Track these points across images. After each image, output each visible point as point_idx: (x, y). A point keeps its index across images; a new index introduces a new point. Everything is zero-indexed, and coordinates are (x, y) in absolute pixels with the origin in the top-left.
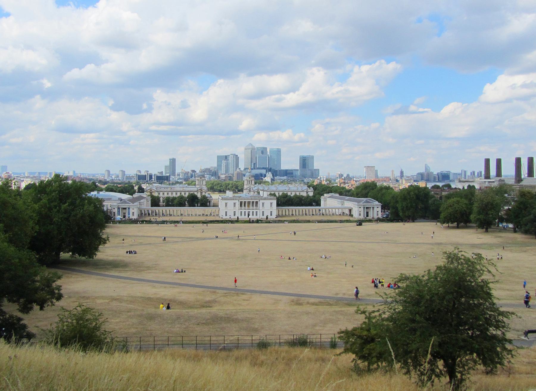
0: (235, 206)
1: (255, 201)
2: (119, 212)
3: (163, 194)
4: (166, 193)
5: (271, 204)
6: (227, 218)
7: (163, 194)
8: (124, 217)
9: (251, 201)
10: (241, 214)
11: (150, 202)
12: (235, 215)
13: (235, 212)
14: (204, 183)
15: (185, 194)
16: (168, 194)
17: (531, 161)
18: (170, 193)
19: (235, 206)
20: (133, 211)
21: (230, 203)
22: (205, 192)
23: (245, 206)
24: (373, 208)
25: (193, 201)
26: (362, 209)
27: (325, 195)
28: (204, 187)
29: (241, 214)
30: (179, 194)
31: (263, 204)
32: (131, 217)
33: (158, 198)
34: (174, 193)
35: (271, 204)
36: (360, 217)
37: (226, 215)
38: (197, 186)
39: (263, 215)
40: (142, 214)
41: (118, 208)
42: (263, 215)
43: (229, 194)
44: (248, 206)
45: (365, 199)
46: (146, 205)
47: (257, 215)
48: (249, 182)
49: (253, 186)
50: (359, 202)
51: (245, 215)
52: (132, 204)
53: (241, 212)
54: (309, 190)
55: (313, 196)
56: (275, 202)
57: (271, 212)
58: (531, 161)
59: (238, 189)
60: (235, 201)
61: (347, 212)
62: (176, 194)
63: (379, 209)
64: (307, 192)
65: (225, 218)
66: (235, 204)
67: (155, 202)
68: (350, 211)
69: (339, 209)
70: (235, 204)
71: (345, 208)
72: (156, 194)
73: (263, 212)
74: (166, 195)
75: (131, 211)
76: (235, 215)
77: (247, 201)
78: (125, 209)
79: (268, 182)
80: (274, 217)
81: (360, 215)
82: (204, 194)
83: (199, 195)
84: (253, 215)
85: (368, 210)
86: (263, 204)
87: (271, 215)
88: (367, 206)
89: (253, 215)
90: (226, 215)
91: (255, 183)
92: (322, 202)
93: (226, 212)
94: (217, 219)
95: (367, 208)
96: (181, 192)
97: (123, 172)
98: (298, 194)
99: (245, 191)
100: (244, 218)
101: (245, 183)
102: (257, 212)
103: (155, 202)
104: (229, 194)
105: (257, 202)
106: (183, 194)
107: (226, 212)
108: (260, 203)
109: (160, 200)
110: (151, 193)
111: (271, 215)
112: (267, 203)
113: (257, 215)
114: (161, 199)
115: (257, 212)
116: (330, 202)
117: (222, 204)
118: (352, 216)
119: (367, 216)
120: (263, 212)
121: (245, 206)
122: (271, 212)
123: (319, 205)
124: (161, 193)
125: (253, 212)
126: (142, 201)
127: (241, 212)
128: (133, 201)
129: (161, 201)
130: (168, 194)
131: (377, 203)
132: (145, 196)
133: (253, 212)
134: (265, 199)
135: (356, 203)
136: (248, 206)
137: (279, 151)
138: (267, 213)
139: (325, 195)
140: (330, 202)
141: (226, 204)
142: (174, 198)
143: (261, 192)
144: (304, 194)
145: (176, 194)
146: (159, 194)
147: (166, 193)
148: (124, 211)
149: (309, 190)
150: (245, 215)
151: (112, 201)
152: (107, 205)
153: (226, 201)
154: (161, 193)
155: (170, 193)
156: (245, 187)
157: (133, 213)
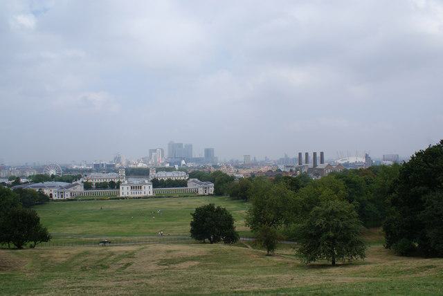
11: (83, 187)
17: (322, 154)
21: (125, 187)
25: (114, 185)
32: (66, 197)
48: (153, 171)
56: (151, 186)
58: (322, 154)
67: (87, 186)
72: (89, 181)
75: (66, 193)
80: (151, 194)
83: (116, 181)
92: (188, 184)
94: (118, 196)
100: (133, 196)
103: (87, 186)
108: (143, 187)
112: (147, 187)
123: (186, 186)
134: (146, 184)
144: (182, 178)
151: (50, 190)
152: (47, 192)
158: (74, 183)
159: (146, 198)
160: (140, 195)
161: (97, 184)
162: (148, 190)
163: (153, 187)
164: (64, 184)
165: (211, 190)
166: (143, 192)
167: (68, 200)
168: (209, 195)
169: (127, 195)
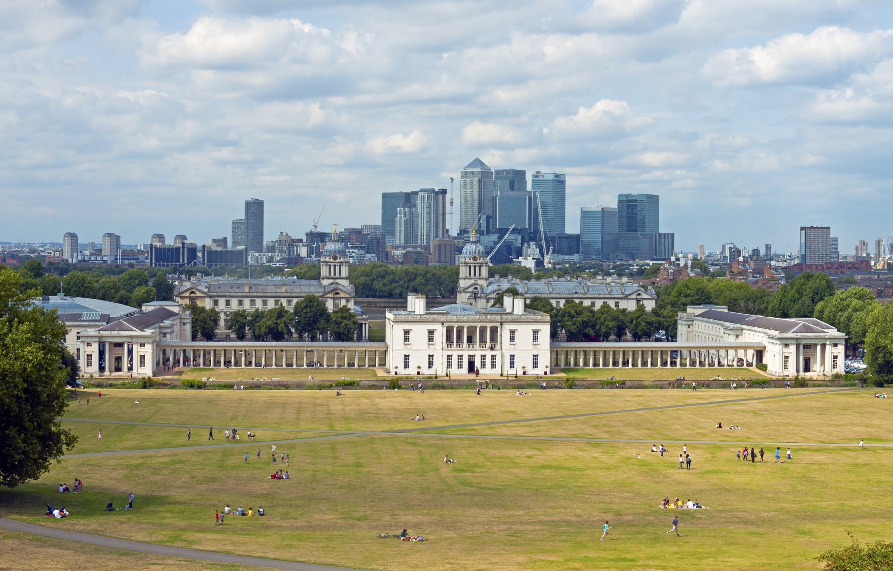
0: (430, 339)
1: (489, 325)
2: (102, 354)
3: (228, 303)
4: (234, 302)
5: (536, 333)
6: (412, 371)
7: (228, 303)
8: (118, 369)
9: (479, 325)
10: (449, 365)
11: (188, 327)
12: (430, 365)
13: (431, 356)
14: (345, 271)
15: (289, 303)
16: (240, 303)
18: (246, 302)
19: (430, 339)
20: (142, 351)
21: (419, 332)
22: (348, 300)
23: (459, 340)
24: (823, 346)
26: (792, 349)
27: (689, 309)
28: (345, 283)
29: (449, 365)
30: (271, 304)
31: (512, 333)
33: (214, 317)
34: (259, 303)
35: (536, 333)
36: (786, 372)
37: (406, 365)
38: (326, 282)
39: (512, 365)
40: (166, 360)
41: (102, 346)
42: (512, 365)
43: (416, 304)
44: (470, 340)
45: (802, 322)
46: (180, 334)
47: (493, 365)
48: (474, 270)
49: (483, 283)
50: (783, 329)
51: (460, 366)
52: (137, 333)
53: (450, 357)
54: (644, 296)
55: (655, 312)
57: (535, 357)
59: (441, 290)
60: (431, 327)
61: (750, 355)
62: (265, 303)
63: (841, 349)
64: (638, 301)
65: (402, 371)
66: (431, 333)
67: (204, 326)
68: (760, 353)
69: (727, 348)
70: (431, 333)
71: (745, 348)
72: (208, 304)
73: (512, 357)
74: (234, 305)
75: (137, 350)
76: (430, 365)
77: (466, 325)
78: (120, 345)
79: (529, 270)
81: (786, 367)
82: (343, 303)
84: (483, 365)
85: (809, 353)
86: (512, 333)
87: (535, 365)
88: (808, 342)
89: (483, 365)
90: (406, 365)
91: (491, 274)
92: (681, 329)
93: (407, 357)
95: (806, 347)
96: (277, 297)
97: (115, 239)
98: (612, 304)
99: (462, 298)
101: (463, 272)
102: (493, 357)
103: (204, 326)
104: (416, 304)
105: (494, 330)
106: (284, 301)
107: (407, 357)
109: (216, 322)
110: (192, 299)
111: (535, 365)
112: (524, 332)
113: (493, 365)
114: (222, 316)
115: (493, 357)
116: (697, 331)
117: (394, 333)
118: (764, 368)
119: (807, 369)
120: (512, 357)
121: (459, 340)
122: (535, 357)
123: (673, 337)
124: (222, 302)
125: (483, 357)
126: (167, 323)
127: (450, 357)
128: (143, 322)
129: (222, 323)
130: (240, 303)
131: (833, 332)
132: (176, 309)
133: (483, 357)
135: (776, 333)
136: (470, 340)
137: (559, 182)
138: (523, 362)
139: (689, 309)
140: (697, 331)
141: (407, 332)
142: (258, 316)
143: (507, 301)
144: (630, 306)
145: (265, 303)
146: (216, 302)
147: (234, 302)
148: (117, 352)
149: (644, 296)
150: (460, 366)
153: (407, 327)
154: (222, 302)
155: (246, 302)
156: (463, 284)
157: (143, 357)
158: (147, 308)
159: (521, 384)
160: (487, 372)
161: (242, 326)
162: (527, 346)
163: (554, 335)
164: (118, 310)
165: (833, 359)
166: (503, 362)
167: (146, 384)
168: (836, 381)
169: (426, 371)
